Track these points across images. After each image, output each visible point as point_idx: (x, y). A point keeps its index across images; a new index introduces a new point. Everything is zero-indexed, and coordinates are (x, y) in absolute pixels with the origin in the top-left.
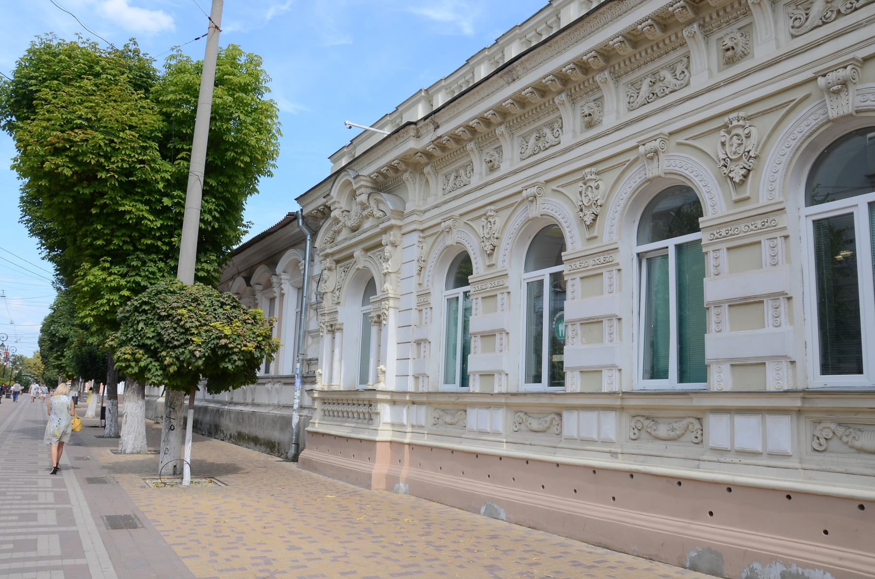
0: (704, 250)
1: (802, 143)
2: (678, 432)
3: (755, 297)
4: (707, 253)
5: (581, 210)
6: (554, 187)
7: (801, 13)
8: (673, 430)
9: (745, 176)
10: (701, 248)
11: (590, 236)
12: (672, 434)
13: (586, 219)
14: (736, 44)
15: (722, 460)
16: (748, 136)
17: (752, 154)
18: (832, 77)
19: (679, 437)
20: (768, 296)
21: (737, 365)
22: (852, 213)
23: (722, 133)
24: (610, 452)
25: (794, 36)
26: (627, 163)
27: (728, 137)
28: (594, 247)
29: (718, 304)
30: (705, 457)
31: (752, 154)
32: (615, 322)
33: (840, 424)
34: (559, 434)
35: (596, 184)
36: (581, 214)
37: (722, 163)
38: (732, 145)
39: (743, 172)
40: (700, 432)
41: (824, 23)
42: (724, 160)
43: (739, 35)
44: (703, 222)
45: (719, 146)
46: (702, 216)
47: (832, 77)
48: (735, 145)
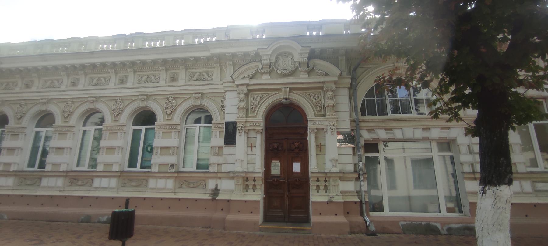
0: (102, 132)
1: (134, 110)
2: (85, 183)
3: (114, 147)
4: (103, 133)
5: (64, 112)
6: (54, 102)
7: (140, 78)
8: (83, 182)
9: (118, 115)
10: (102, 131)
11: (65, 121)
12: (83, 184)
13: (65, 115)
14: (124, 79)
15: (97, 190)
16: (121, 104)
17: (121, 110)
18: (142, 97)
19: (85, 184)
20: (117, 147)
21: (106, 165)
22: (142, 130)
23: (114, 102)
24: (59, 190)
25: (138, 83)
26: (84, 101)
27: (116, 103)
28: (66, 125)
29: (103, 148)
30: (91, 190)
31: (121, 110)
32: (69, 149)
33: (129, 180)
34: (40, 185)
35: (71, 105)
36: (63, 113)
37: (113, 110)
38: (116, 106)
39: (118, 113)
40: (91, 183)
41: (145, 83)
42: (113, 109)
43: (125, 77)
44: (104, 124)
45: (113, 105)
46: (104, 123)
47: (142, 97)
48: (117, 106)
